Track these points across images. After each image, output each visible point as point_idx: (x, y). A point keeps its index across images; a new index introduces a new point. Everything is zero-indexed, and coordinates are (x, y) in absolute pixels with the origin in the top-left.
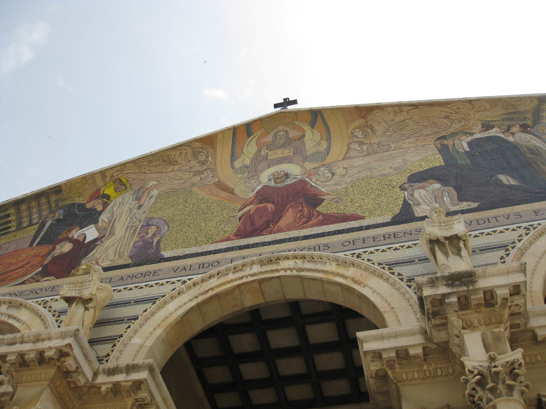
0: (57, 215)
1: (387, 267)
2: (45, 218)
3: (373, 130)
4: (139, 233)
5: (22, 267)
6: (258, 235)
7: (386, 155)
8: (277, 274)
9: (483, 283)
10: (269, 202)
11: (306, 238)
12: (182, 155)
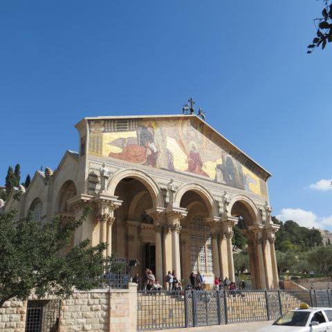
11: (201, 179)
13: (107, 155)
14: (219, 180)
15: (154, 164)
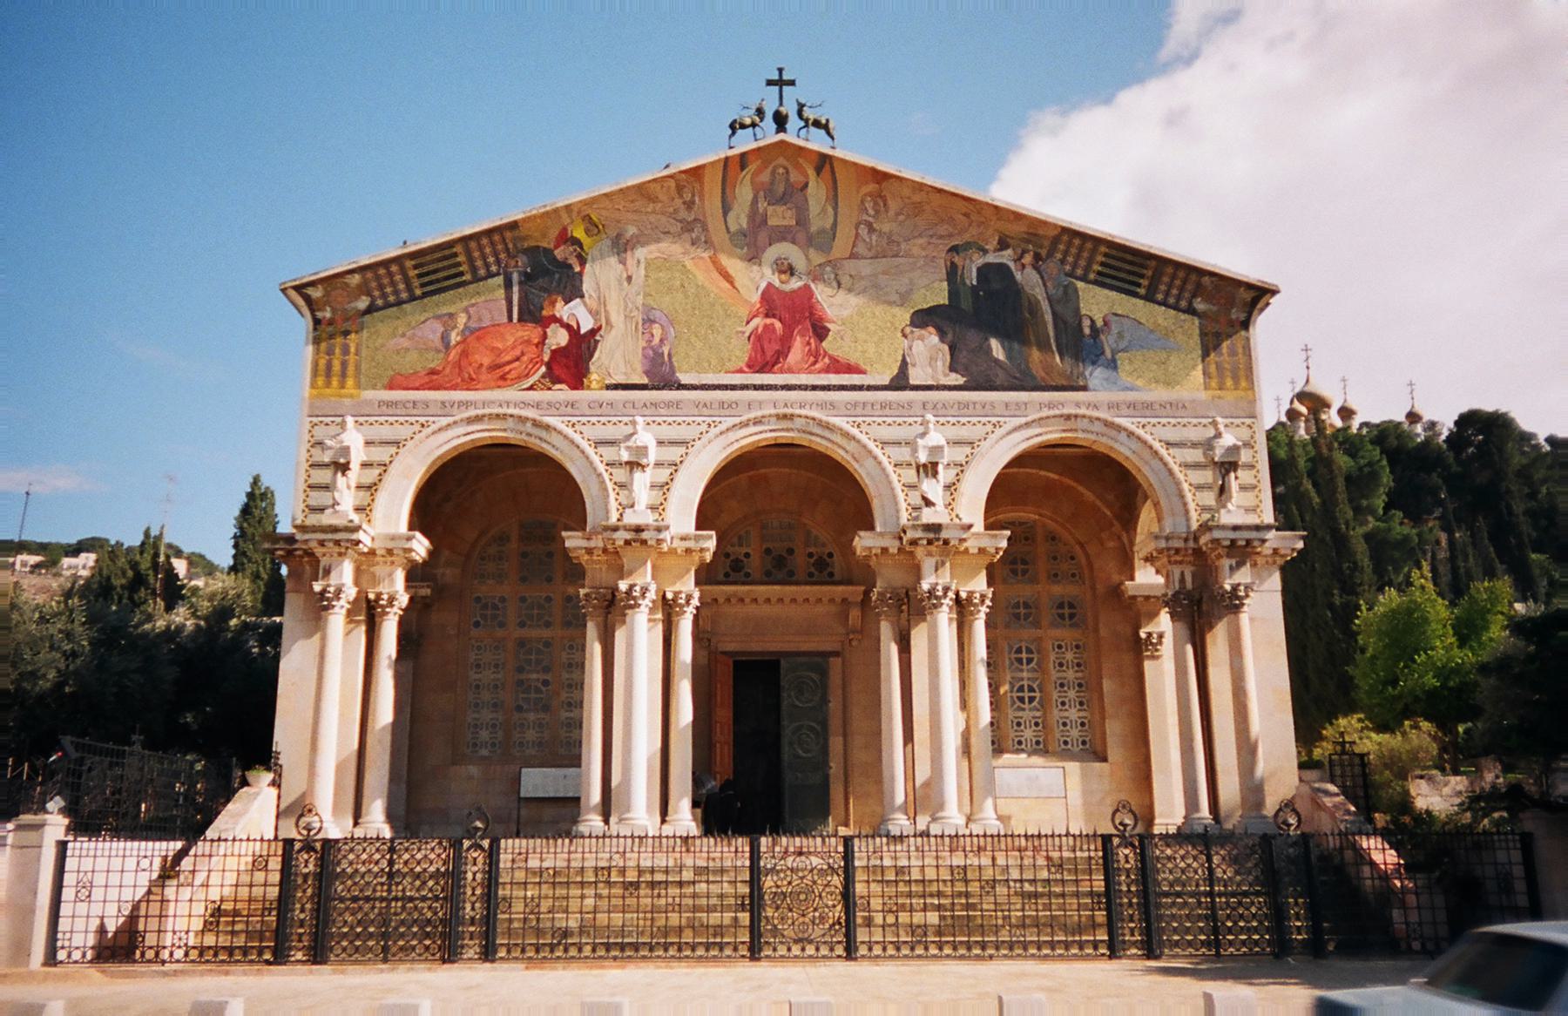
3: (885, 205)
5: (518, 359)
6: (770, 371)
9: (944, 535)
10: (774, 316)
11: (814, 388)
14: (916, 377)
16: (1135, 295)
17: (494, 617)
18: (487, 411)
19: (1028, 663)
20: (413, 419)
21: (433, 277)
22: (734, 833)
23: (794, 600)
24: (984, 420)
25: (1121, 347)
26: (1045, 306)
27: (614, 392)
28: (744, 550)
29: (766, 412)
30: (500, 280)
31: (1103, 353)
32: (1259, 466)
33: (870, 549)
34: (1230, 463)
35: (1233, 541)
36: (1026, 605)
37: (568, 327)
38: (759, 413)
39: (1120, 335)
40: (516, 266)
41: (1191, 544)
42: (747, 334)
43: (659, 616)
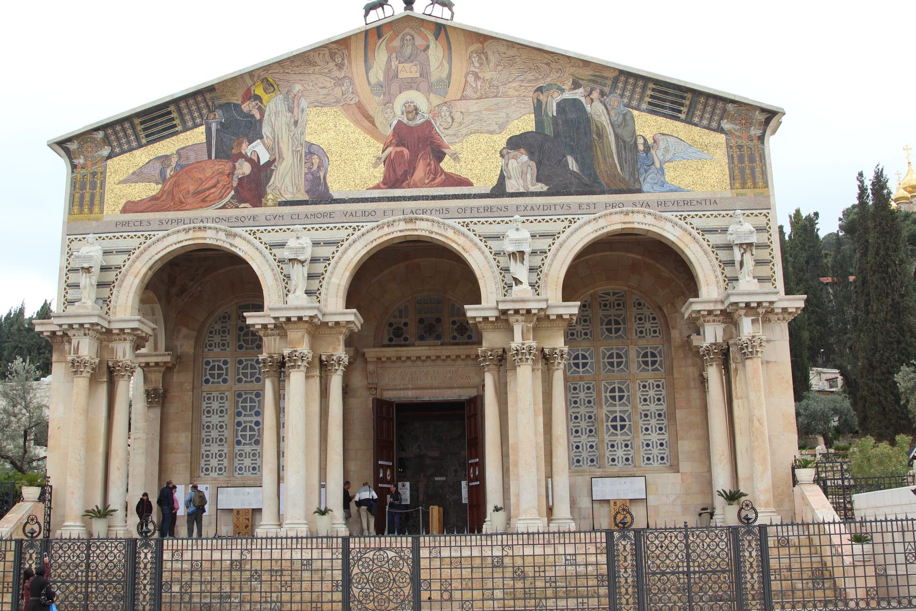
0: (217, 116)
1: (484, 239)
2: (207, 119)
4: (305, 163)
5: (214, 186)
6: (400, 187)
7: (495, 102)
8: (416, 233)
10: (403, 145)
11: (434, 198)
12: (321, 56)
13: (117, 211)
14: (511, 186)
15: (257, 199)
16: (677, 119)
17: (219, 376)
18: (192, 225)
19: (620, 400)
20: (139, 234)
21: (155, 130)
22: (399, 534)
23: (438, 357)
24: (562, 217)
25: (668, 157)
26: (609, 130)
27: (284, 208)
28: (403, 321)
29: (396, 218)
30: (202, 129)
31: (653, 163)
32: (773, 246)
33: (474, 318)
34: (746, 244)
35: (748, 305)
36: (619, 356)
37: (250, 160)
38: (391, 219)
39: (667, 150)
40: (215, 118)
41: (720, 307)
42: (383, 160)
43: (317, 373)
